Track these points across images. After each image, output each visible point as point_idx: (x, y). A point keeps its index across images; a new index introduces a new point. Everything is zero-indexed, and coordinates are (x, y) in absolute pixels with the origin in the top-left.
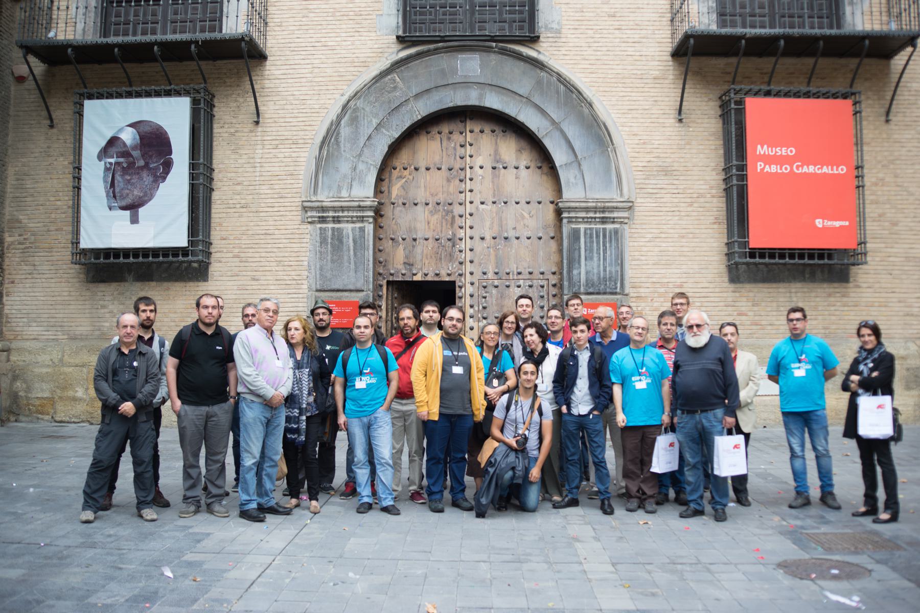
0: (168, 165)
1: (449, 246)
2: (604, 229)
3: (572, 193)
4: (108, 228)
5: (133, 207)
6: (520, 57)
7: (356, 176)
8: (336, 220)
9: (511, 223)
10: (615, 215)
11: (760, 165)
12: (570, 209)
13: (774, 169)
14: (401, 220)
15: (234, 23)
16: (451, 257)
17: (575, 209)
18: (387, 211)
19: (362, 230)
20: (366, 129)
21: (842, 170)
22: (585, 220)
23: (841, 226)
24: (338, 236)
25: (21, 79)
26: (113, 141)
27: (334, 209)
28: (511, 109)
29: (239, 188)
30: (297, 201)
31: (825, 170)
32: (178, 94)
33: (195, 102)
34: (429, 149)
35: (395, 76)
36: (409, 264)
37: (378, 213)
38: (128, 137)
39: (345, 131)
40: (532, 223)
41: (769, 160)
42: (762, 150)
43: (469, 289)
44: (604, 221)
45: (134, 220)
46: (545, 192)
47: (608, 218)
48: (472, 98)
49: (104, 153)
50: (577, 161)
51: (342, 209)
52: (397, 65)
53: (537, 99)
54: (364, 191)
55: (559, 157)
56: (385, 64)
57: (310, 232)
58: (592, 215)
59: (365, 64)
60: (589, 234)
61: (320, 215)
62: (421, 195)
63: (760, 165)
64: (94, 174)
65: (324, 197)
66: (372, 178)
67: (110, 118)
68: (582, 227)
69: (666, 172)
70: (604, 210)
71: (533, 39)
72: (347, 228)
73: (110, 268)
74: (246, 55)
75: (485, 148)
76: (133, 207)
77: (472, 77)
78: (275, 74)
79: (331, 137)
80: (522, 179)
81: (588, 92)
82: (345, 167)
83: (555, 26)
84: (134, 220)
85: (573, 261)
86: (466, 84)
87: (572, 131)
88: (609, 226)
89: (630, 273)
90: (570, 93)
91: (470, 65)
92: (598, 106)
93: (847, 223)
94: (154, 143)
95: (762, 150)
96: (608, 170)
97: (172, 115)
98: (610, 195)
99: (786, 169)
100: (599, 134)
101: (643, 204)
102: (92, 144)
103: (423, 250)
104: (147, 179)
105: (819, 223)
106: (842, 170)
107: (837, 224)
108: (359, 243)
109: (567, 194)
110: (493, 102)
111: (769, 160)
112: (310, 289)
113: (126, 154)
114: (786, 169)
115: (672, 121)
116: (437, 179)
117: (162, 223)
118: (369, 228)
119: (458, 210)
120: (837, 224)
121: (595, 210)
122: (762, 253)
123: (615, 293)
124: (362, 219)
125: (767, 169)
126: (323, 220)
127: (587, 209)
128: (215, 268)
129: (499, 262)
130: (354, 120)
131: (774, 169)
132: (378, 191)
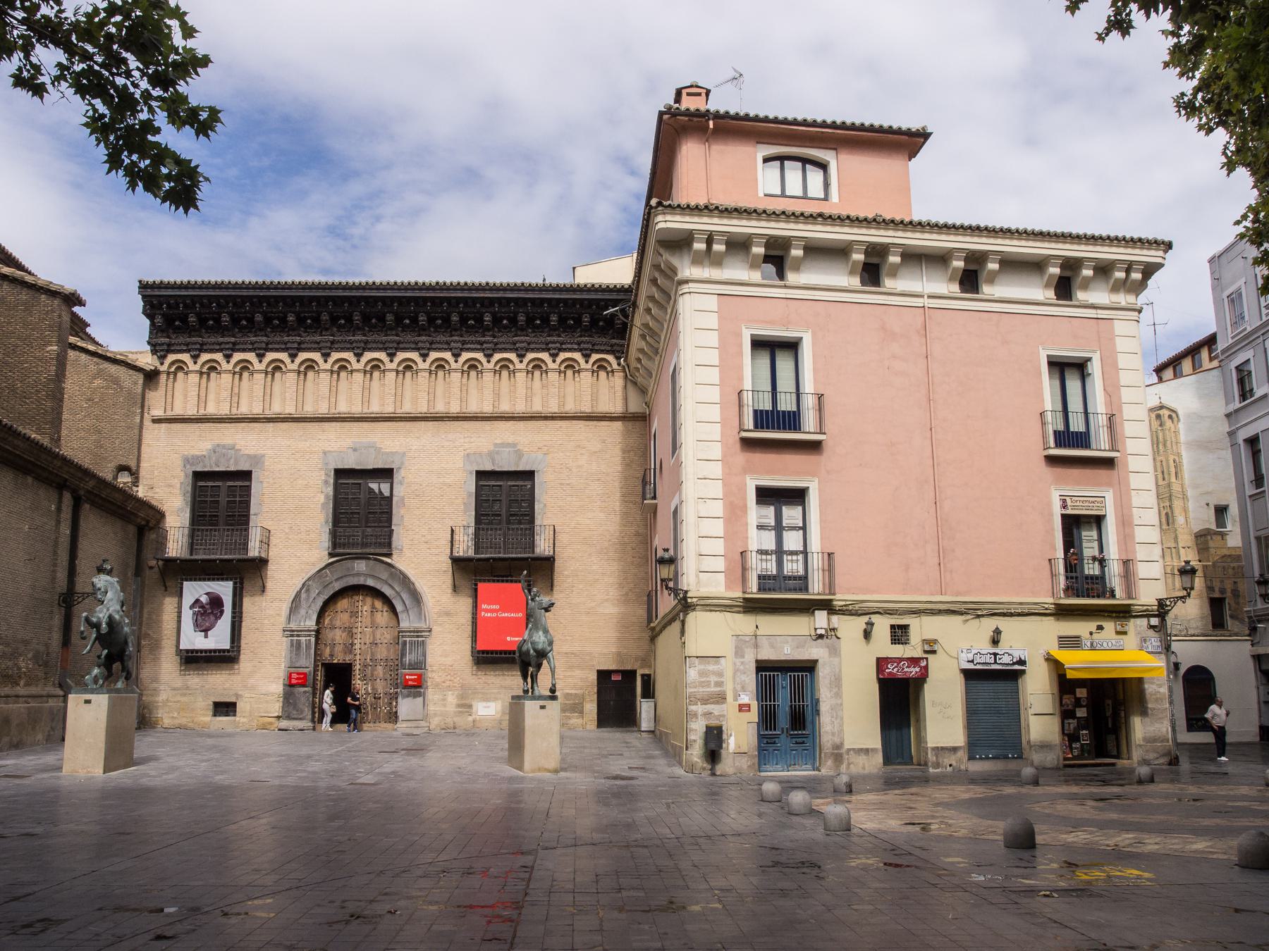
0: (222, 612)
1: (349, 648)
3: (404, 624)
4: (193, 640)
5: (206, 631)
6: (383, 562)
7: (307, 616)
9: (378, 636)
14: (328, 635)
15: (254, 551)
16: (351, 652)
18: (323, 631)
20: (313, 595)
21: (520, 615)
24: (299, 642)
25: (151, 568)
26: (197, 601)
28: (378, 586)
30: (281, 627)
32: (227, 580)
33: (235, 583)
34: (343, 603)
36: (331, 655)
37: (318, 632)
38: (204, 599)
39: (303, 595)
40: (388, 636)
41: (487, 611)
42: (484, 606)
43: (358, 667)
45: (206, 636)
46: (394, 623)
47: (420, 638)
48: (361, 581)
49: (192, 607)
50: (406, 610)
53: (390, 582)
54: (311, 623)
55: (399, 608)
56: (323, 565)
57: (285, 642)
59: (313, 564)
60: (411, 643)
61: (290, 633)
62: (338, 623)
64: (188, 616)
65: (293, 626)
66: (315, 617)
67: (195, 591)
69: (448, 614)
71: (389, 555)
73: (194, 660)
74: (260, 564)
75: (365, 605)
76: (206, 631)
77: (361, 571)
78: (272, 570)
79: (298, 595)
80: (383, 617)
81: (413, 579)
82: (303, 612)
84: (206, 636)
85: (403, 655)
86: (358, 574)
87: (405, 596)
89: (429, 660)
90: (405, 581)
91: (361, 566)
92: (417, 585)
94: (216, 602)
95: (484, 606)
97: (225, 589)
98: (422, 625)
99: (495, 615)
100: (416, 597)
101: (436, 629)
102: (188, 600)
103: (338, 649)
104: (212, 618)
106: (520, 615)
108: (308, 646)
109: (402, 625)
110: (370, 582)
111: (487, 611)
113: (202, 607)
114: (495, 615)
115: (450, 591)
116: (345, 617)
117: (218, 638)
118: (313, 640)
119: (354, 630)
122: (483, 652)
128: (242, 657)
129: (372, 654)
130: (308, 590)
132: (318, 622)
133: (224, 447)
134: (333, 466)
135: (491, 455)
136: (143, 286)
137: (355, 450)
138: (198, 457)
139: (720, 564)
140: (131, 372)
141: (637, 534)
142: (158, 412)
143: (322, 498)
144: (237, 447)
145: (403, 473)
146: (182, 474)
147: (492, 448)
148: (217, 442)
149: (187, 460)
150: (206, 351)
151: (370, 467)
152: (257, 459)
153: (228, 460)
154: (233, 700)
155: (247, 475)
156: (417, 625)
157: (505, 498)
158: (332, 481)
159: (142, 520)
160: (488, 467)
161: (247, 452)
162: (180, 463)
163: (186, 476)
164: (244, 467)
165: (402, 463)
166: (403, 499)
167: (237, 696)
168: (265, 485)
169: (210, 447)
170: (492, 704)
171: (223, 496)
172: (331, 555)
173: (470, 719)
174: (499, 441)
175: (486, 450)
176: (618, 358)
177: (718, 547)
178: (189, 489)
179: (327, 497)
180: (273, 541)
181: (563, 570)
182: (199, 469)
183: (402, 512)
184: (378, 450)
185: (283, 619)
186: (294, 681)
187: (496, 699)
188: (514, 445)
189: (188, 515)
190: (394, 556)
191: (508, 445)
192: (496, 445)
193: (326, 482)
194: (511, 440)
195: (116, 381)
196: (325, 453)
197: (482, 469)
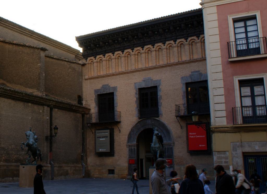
2: (170, 147)
6: (155, 119)
8: (131, 147)
10: (171, 145)
11: (190, 136)
12: (164, 144)
13: (192, 137)
17: (165, 144)
19: (135, 148)
21: (204, 136)
22: (167, 146)
23: (204, 146)
24: (132, 149)
27: (131, 145)
29: (118, 142)
31: (201, 136)
35: (139, 124)
41: (191, 135)
42: (190, 134)
44: (170, 146)
51: (132, 145)
52: (139, 122)
58: (168, 145)
60: (167, 148)
63: (190, 136)
65: (129, 144)
66: (136, 140)
68: (166, 147)
70: (169, 144)
71: (158, 117)
72: (133, 148)
81: (166, 125)
83: (161, 114)
88: (171, 147)
91: (149, 121)
93: (205, 145)
95: (190, 134)
101: (176, 143)
105: (200, 146)
106: (204, 136)
107: (203, 146)
111: (191, 135)
112: (128, 158)
114: (194, 137)
120: (203, 146)
121: (168, 144)
123: (172, 158)
124: (135, 147)
125: (191, 137)
126: (129, 147)
127: (167, 144)
128: (115, 155)
131: (192, 137)
133: (105, 85)
134: (138, 87)
135: (190, 76)
136: (76, 37)
137: (144, 81)
138: (98, 90)
139: (224, 114)
140: (78, 65)
142: (87, 77)
143: (135, 99)
144: (109, 85)
145: (160, 87)
146: (95, 96)
147: (190, 73)
148: (103, 84)
149: (96, 91)
150: (98, 55)
151: (150, 86)
152: (115, 88)
155: (112, 94)
158: (138, 93)
159: (85, 112)
161: (112, 86)
162: (93, 92)
163: (96, 96)
164: (111, 91)
165: (160, 83)
166: (161, 96)
168: (118, 97)
169: (101, 86)
171: (106, 100)
172: (139, 118)
174: (192, 71)
175: (188, 75)
177: (223, 107)
179: (137, 98)
182: (99, 94)
183: (161, 101)
184: (152, 80)
185: (126, 141)
188: (199, 71)
189: (97, 109)
190: (160, 117)
191: (197, 72)
192: (192, 72)
193: (136, 93)
194: (197, 70)
195: (74, 69)
196: (135, 83)
197: (187, 82)
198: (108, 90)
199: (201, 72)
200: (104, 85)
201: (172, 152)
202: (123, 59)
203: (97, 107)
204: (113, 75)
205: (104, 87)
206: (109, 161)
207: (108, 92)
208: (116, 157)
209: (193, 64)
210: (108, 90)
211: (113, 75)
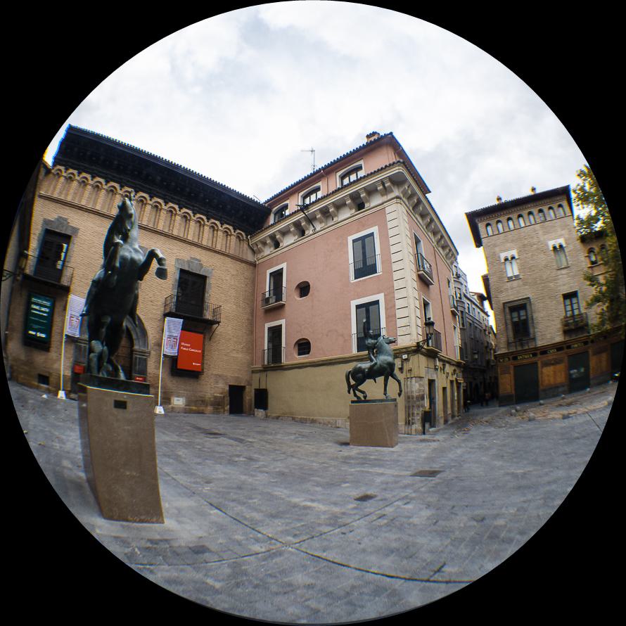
3: (136, 347)
12: (136, 351)
21: (200, 351)
42: (183, 344)
55: (134, 336)
81: (143, 321)
95: (183, 344)
96: (145, 340)
100: (144, 333)
106: (200, 351)
114: (187, 349)
121: (142, 352)
135: (188, 262)
141: (248, 319)
148: (60, 215)
152: (76, 230)
153: (63, 227)
154: (47, 375)
156: (142, 349)
157: (192, 287)
160: (187, 268)
167: (50, 374)
170: (181, 399)
173: (170, 406)
175: (186, 260)
176: (247, 236)
178: (41, 237)
180: (74, 281)
181: (220, 330)
186: (76, 371)
187: (182, 397)
188: (200, 261)
191: (197, 260)
194: (198, 258)
198: (64, 228)
199: (201, 262)
200: (61, 217)
201: (146, 366)
202: (103, 192)
203: (38, 250)
204: (80, 208)
205: (61, 220)
206: (39, 358)
207: (63, 232)
208: (53, 354)
209: (195, 248)
210: (64, 228)
211: (80, 208)
